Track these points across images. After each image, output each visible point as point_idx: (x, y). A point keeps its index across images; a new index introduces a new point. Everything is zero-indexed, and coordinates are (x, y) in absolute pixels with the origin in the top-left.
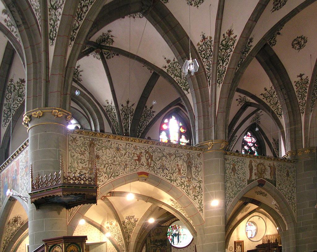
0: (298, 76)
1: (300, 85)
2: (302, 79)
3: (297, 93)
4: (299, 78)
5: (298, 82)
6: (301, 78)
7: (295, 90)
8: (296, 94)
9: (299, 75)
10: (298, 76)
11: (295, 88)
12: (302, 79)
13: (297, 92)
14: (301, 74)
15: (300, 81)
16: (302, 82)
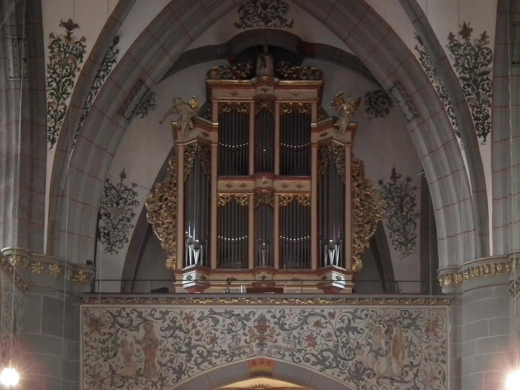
0: (63, 24)
1: (60, 51)
2: (68, 37)
3: (49, 72)
4: (62, 32)
5: (59, 40)
6: (69, 34)
7: (47, 61)
8: (47, 75)
9: (66, 20)
10: (63, 24)
11: (47, 53)
12: (68, 37)
13: (49, 67)
14: (70, 21)
15: (63, 41)
16: (68, 46)
